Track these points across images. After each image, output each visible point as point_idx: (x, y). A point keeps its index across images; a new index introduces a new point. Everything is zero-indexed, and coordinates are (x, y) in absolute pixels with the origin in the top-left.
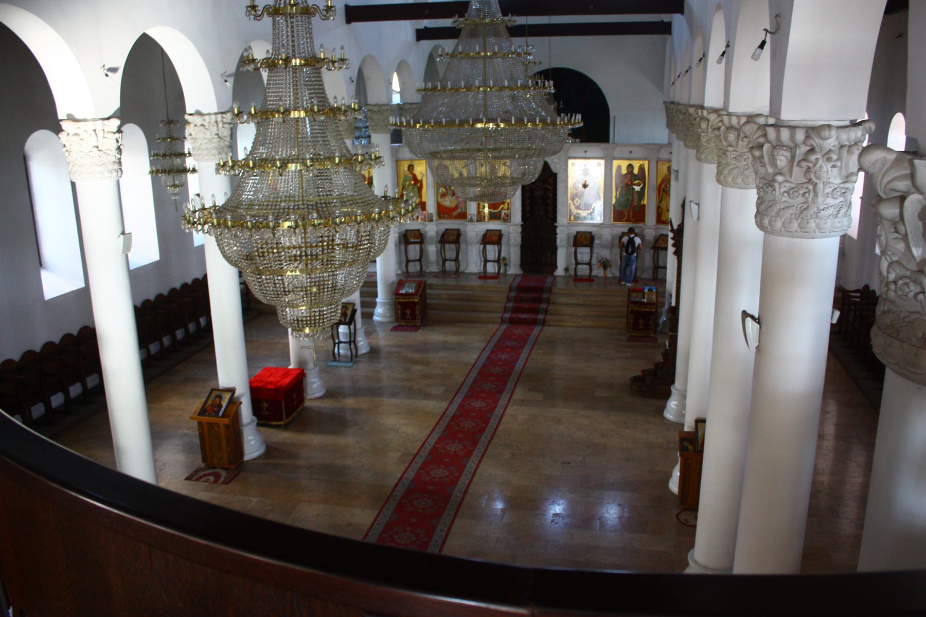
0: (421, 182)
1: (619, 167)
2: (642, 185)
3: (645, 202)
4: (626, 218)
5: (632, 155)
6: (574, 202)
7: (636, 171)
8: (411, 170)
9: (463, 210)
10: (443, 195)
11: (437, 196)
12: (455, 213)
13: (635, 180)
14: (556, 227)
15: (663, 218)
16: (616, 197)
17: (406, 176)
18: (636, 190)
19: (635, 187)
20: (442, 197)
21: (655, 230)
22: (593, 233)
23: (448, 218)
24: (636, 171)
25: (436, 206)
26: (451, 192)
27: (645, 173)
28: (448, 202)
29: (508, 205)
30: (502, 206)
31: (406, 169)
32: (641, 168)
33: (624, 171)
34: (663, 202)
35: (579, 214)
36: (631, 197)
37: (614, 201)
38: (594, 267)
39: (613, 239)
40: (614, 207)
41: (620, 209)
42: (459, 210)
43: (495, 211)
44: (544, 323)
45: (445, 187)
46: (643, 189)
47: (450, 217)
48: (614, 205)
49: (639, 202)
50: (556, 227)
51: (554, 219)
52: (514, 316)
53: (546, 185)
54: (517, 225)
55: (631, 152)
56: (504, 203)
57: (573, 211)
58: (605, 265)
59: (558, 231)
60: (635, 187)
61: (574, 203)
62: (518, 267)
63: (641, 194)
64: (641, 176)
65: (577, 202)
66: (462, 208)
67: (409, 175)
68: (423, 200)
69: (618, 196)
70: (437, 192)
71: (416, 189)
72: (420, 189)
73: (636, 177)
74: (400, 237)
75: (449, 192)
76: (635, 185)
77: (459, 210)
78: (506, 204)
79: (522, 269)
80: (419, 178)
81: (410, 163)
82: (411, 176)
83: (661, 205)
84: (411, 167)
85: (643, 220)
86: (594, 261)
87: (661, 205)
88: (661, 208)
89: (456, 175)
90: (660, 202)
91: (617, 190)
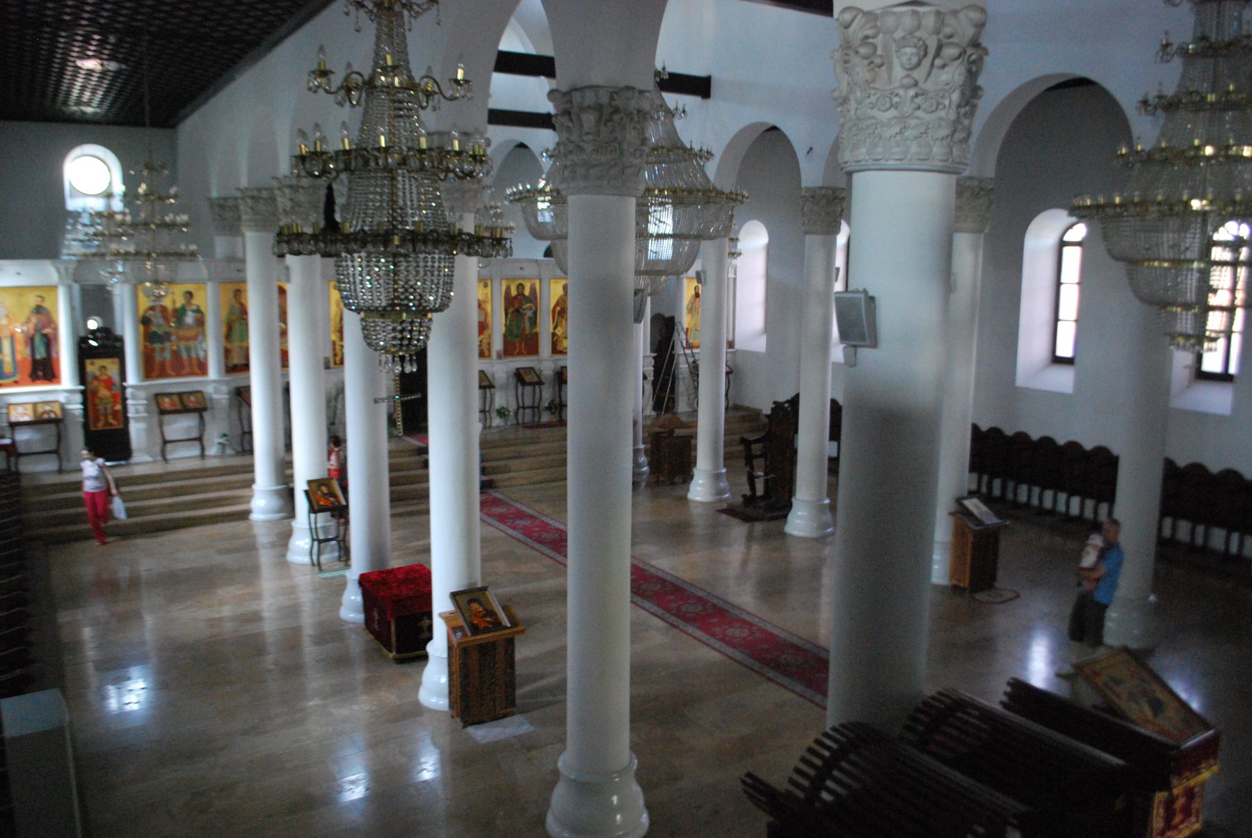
2: (534, 309)
3: (538, 330)
7: (527, 292)
13: (527, 302)
16: (506, 325)
21: (554, 361)
24: (527, 292)
31: (231, 295)
32: (533, 289)
33: (514, 292)
34: (559, 328)
39: (508, 378)
46: (535, 313)
58: (502, 413)
63: (534, 321)
64: (533, 298)
73: (528, 300)
81: (237, 287)
83: (557, 331)
87: (557, 331)
88: (556, 335)
90: (555, 328)
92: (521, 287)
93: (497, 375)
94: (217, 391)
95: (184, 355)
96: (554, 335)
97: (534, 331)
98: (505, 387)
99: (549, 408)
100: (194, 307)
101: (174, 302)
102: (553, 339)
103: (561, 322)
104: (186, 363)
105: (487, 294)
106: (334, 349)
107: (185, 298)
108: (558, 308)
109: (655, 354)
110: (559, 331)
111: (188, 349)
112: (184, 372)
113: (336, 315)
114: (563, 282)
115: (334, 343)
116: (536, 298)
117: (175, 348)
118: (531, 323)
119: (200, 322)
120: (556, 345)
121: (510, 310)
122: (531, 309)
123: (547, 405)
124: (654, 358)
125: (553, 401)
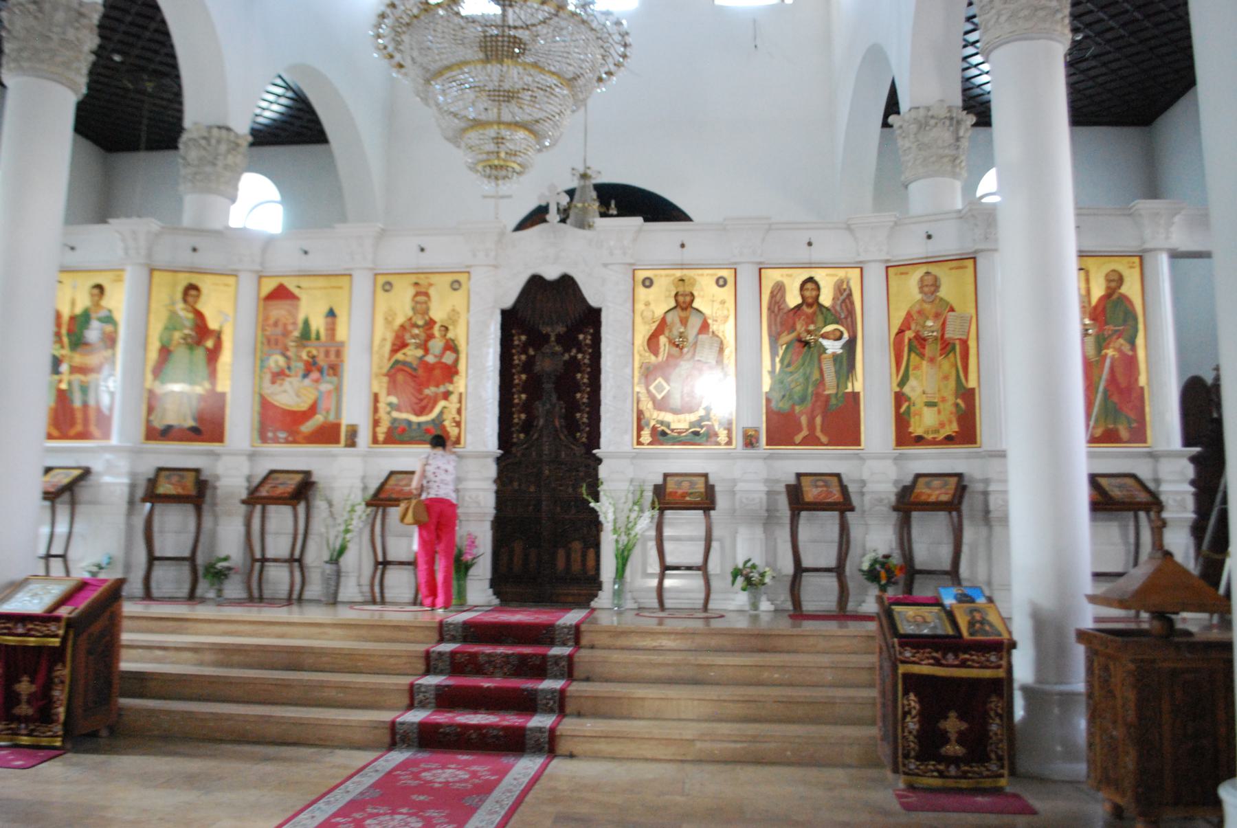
0: (218, 336)
1: (779, 290)
2: (846, 336)
3: (858, 386)
4: (805, 433)
5: (816, 254)
6: (652, 388)
7: (826, 299)
8: (190, 299)
9: (332, 418)
10: (279, 375)
11: (261, 378)
12: (308, 427)
13: (826, 324)
14: (599, 461)
15: (916, 429)
16: (772, 372)
17: (173, 315)
18: (829, 351)
19: (825, 343)
20: (273, 382)
22: (712, 481)
23: (287, 442)
25: (257, 408)
26: (301, 365)
27: (852, 303)
28: (291, 395)
29: (460, 402)
30: (442, 403)
32: (844, 295)
33: (793, 299)
34: (912, 382)
35: (668, 426)
36: (816, 375)
37: (766, 387)
38: (715, 584)
39: (769, 493)
40: (768, 401)
41: (785, 406)
42: (319, 419)
43: (423, 419)
44: (549, 745)
45: (284, 355)
46: (851, 346)
47: (295, 438)
48: (766, 393)
49: (838, 386)
50: (599, 461)
51: (594, 439)
52: (442, 718)
53: (574, 351)
54: (483, 455)
55: (810, 244)
56: (446, 395)
57: (647, 415)
58: (749, 578)
59: (603, 471)
60: (825, 343)
61: (648, 391)
62: (487, 584)
63: (846, 362)
64: (844, 311)
65: (660, 388)
66: (328, 411)
67: (183, 314)
68: (220, 389)
69: (778, 366)
70: (262, 367)
71: (200, 354)
72: (213, 356)
74: (133, 487)
75: (293, 364)
76: (824, 336)
77: (319, 419)
78: (454, 398)
79: (495, 593)
80: (213, 324)
82: (191, 316)
84: (193, 292)
85: (856, 441)
86: (714, 566)
88: (908, 399)
89: (318, 323)
90: (902, 383)
91: (774, 353)
92: (809, 286)
93: (740, 486)
94: (110, 468)
95: (77, 403)
96: (900, 398)
97: (849, 389)
98: (769, 520)
99: (872, 575)
100: (102, 313)
101: (73, 303)
102: (898, 405)
103: (916, 368)
104: (79, 416)
105: (723, 302)
106: (376, 410)
107: (92, 295)
108: (909, 334)
109: (1196, 450)
110: (913, 389)
111: (84, 389)
112: (73, 432)
113: (384, 339)
114: (921, 271)
115: (376, 398)
116: (851, 313)
117: (64, 386)
118: (838, 373)
119: (110, 341)
120: (907, 424)
121: (786, 338)
122: (840, 338)
123: (866, 566)
124: (1194, 459)
125: (887, 557)
